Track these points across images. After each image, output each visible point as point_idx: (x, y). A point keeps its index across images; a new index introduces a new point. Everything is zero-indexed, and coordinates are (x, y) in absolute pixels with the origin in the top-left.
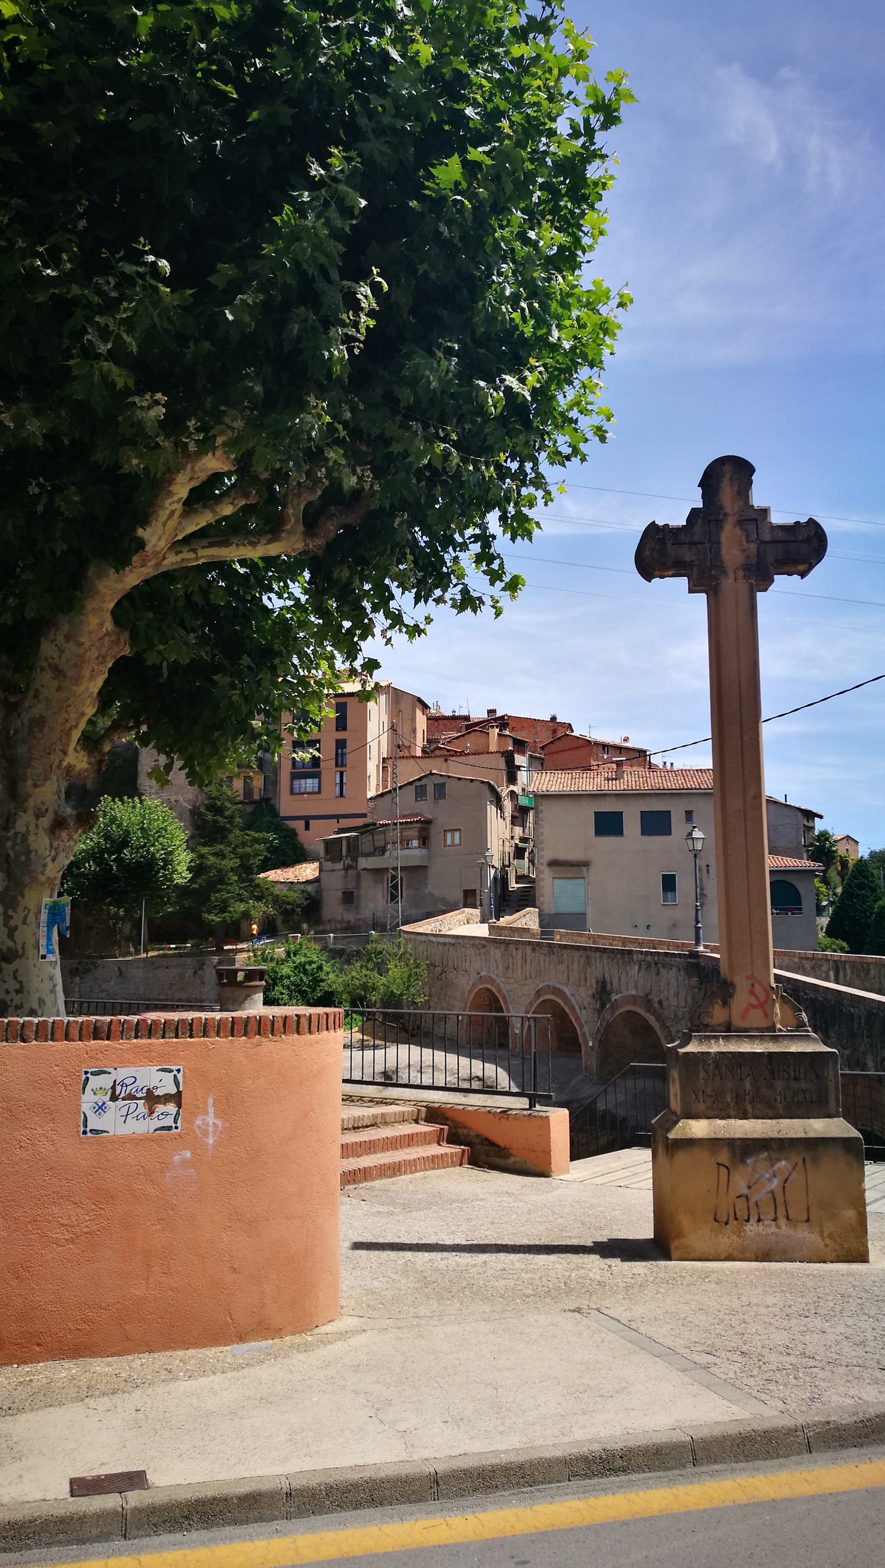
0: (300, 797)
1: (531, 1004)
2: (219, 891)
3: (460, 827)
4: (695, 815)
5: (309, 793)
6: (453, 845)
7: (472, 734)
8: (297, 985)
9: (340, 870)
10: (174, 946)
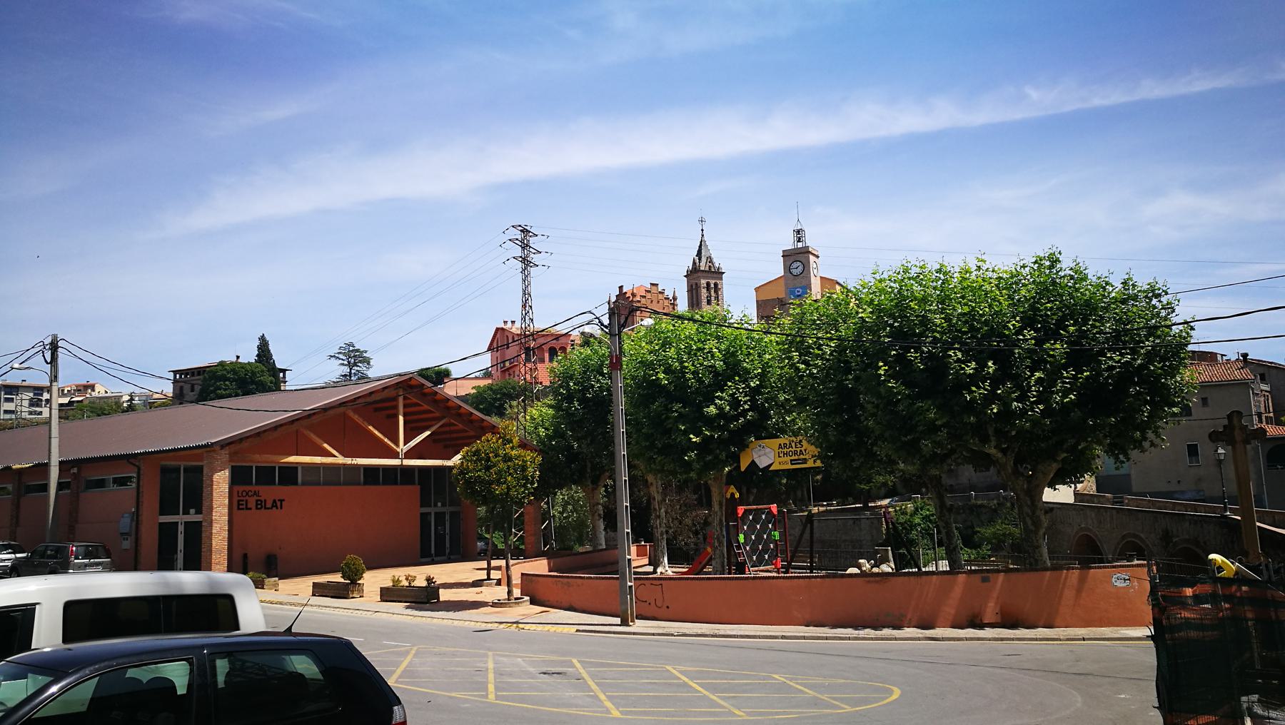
1: (1118, 544)
4: (1209, 401)
8: (926, 530)
10: (825, 503)
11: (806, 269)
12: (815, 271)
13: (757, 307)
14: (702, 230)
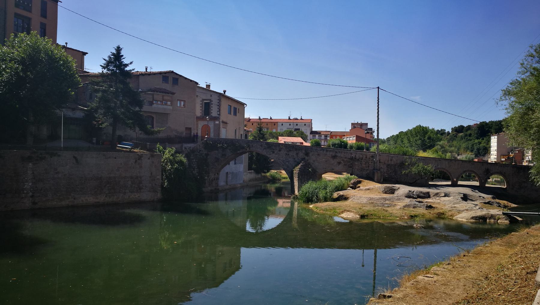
6: (180, 107)
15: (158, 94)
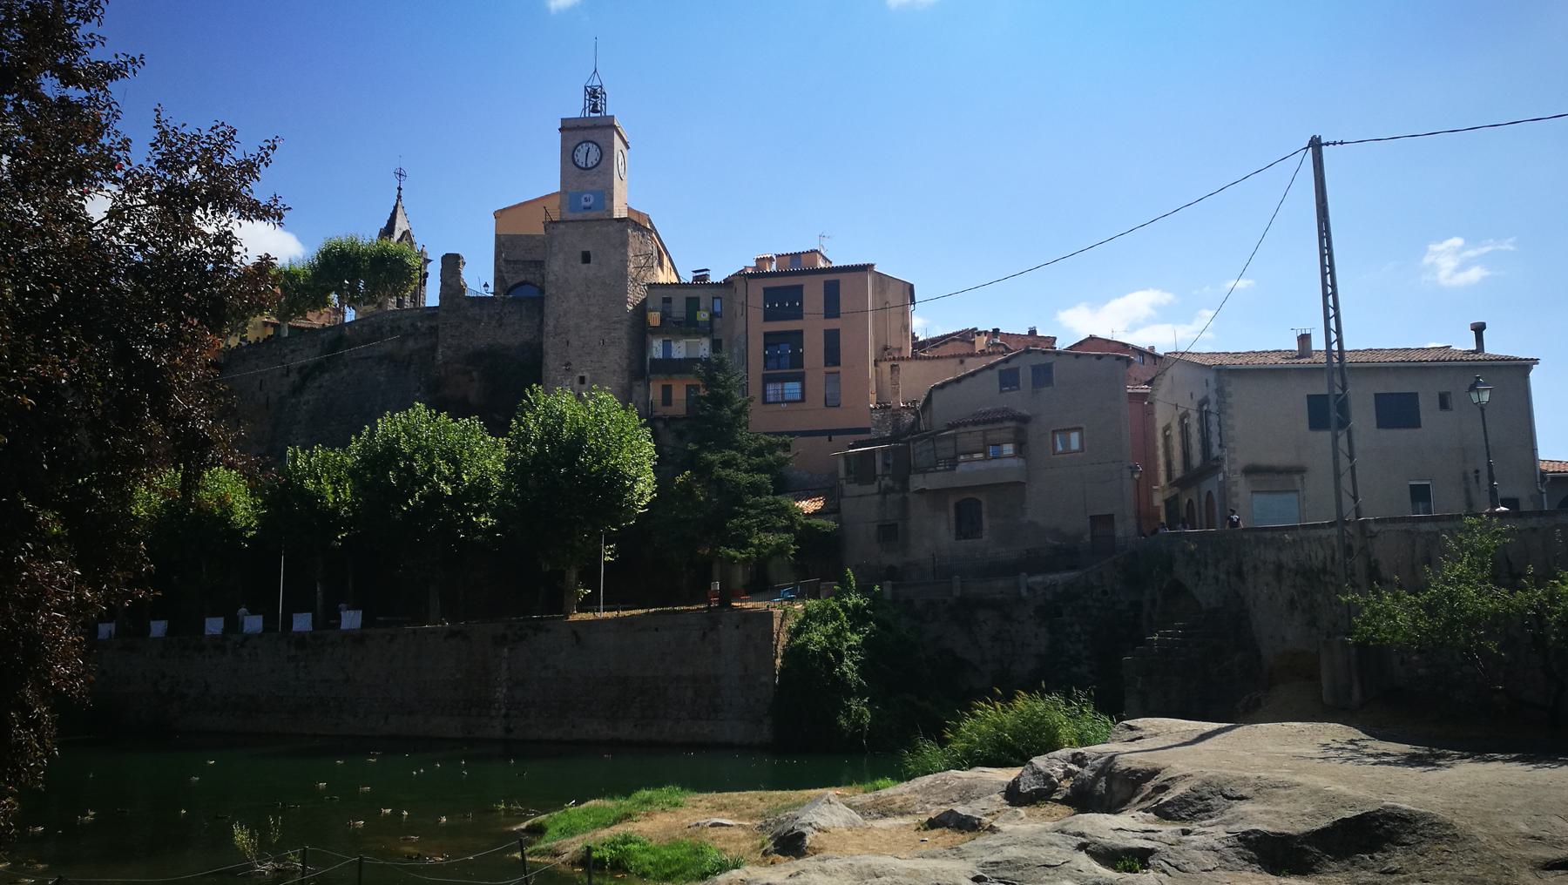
0: (776, 407)
2: (736, 515)
3: (1081, 425)
5: (788, 402)
7: (950, 344)
9: (873, 494)
11: (604, 158)
12: (621, 168)
13: (497, 246)
14: (400, 189)
15: (970, 432)
